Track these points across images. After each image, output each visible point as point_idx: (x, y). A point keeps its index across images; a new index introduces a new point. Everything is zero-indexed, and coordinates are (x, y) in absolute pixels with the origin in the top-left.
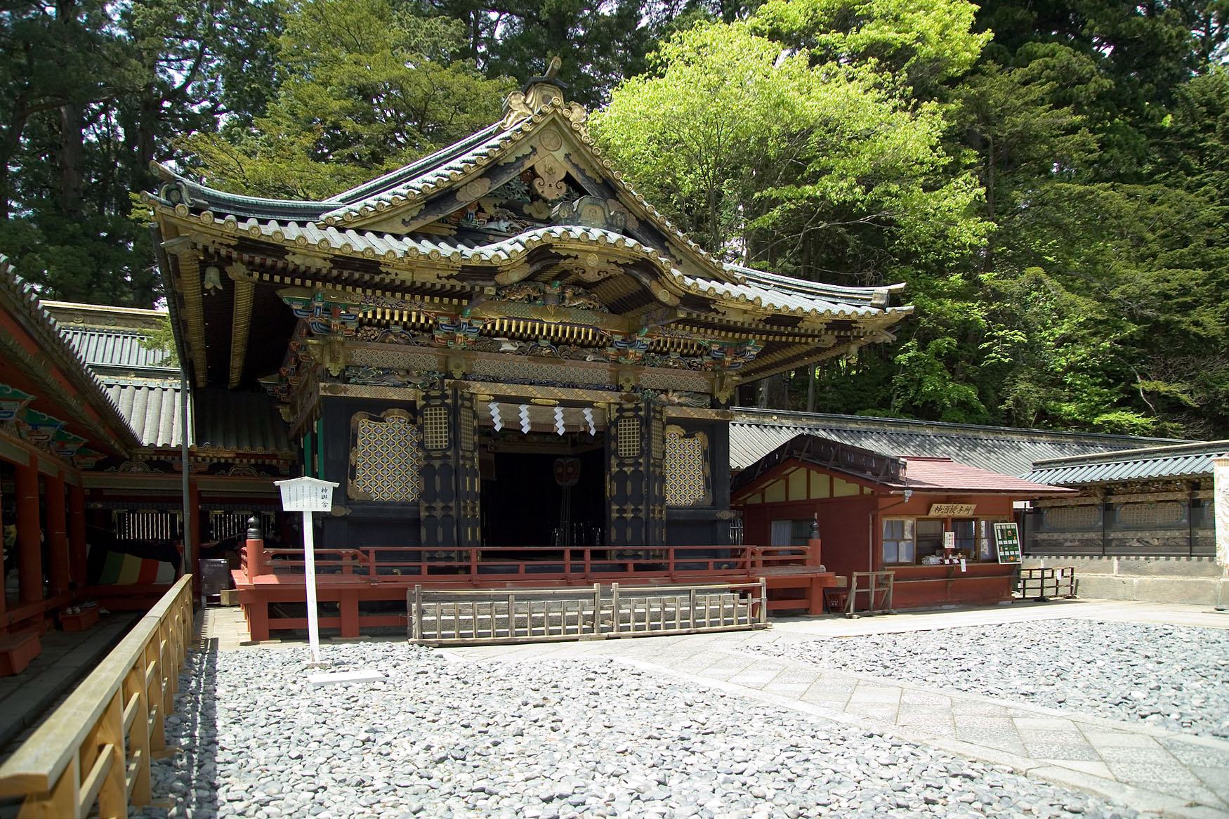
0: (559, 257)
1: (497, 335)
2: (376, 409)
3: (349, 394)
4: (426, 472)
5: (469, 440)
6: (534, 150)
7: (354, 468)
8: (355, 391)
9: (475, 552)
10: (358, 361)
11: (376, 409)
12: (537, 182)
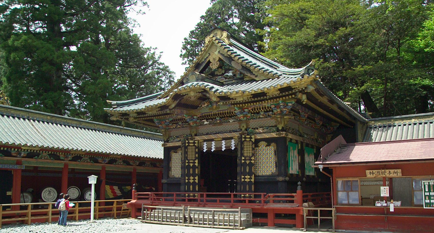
0: (183, 96)
3: (168, 146)
10: (171, 135)
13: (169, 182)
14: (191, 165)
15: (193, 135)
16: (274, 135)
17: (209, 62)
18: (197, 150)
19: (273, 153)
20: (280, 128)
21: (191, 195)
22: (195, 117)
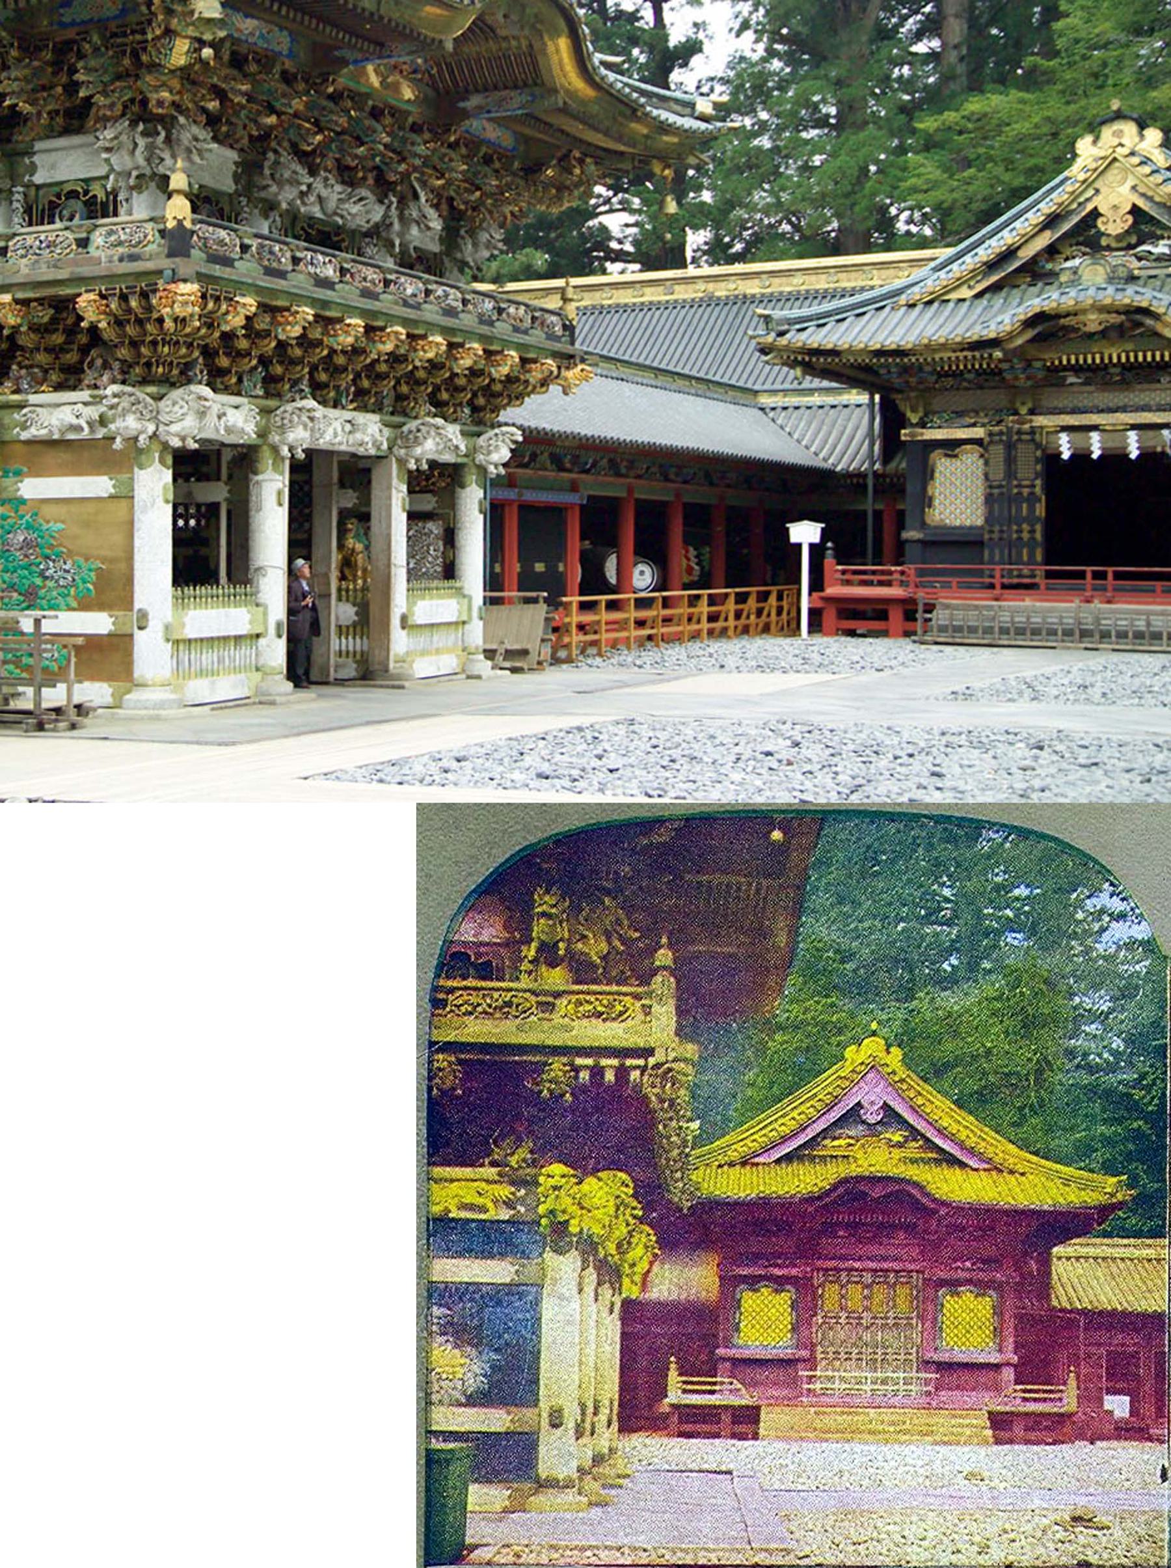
1: (1065, 369)
2: (951, 447)
4: (989, 499)
5: (1029, 472)
7: (931, 499)
9: (1040, 570)
11: (951, 447)
12: (1099, 222)
13: (929, 538)
17: (1095, 214)
18: (1039, 453)
21: (1026, 572)
22: (1038, 364)
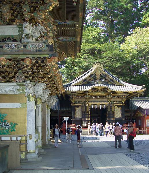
1: (92, 96)
6: (96, 72)
8: (75, 105)
14: (88, 113)
15: (87, 102)
16: (121, 104)
19: (120, 110)
20: (123, 103)
